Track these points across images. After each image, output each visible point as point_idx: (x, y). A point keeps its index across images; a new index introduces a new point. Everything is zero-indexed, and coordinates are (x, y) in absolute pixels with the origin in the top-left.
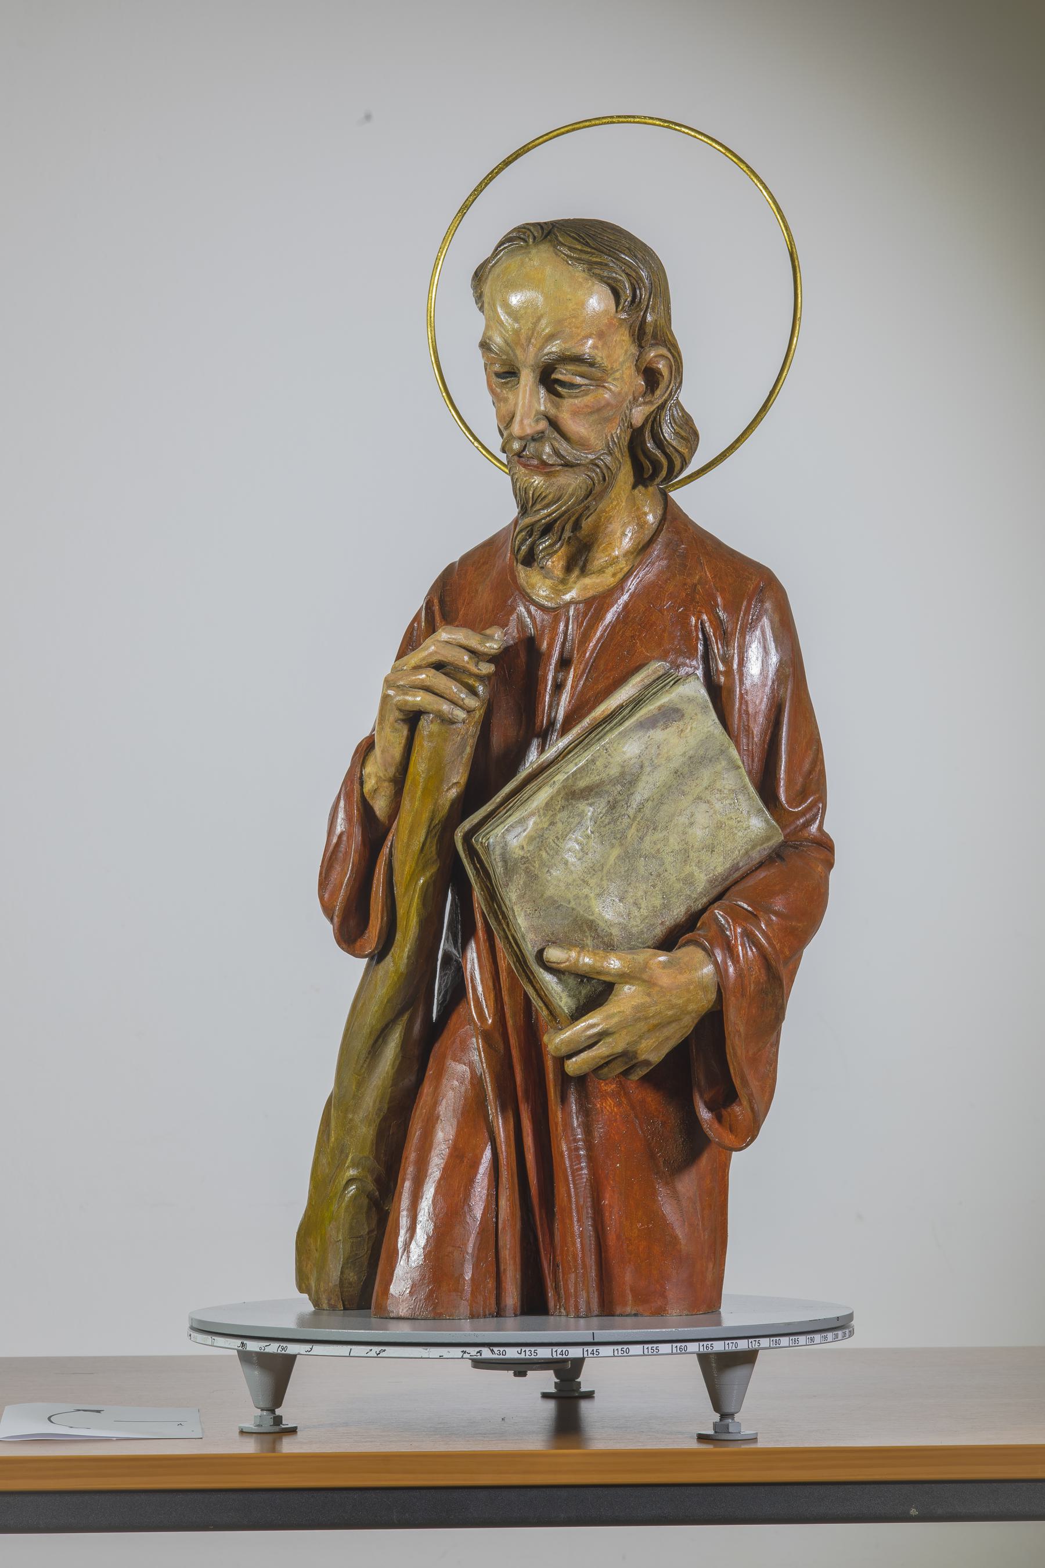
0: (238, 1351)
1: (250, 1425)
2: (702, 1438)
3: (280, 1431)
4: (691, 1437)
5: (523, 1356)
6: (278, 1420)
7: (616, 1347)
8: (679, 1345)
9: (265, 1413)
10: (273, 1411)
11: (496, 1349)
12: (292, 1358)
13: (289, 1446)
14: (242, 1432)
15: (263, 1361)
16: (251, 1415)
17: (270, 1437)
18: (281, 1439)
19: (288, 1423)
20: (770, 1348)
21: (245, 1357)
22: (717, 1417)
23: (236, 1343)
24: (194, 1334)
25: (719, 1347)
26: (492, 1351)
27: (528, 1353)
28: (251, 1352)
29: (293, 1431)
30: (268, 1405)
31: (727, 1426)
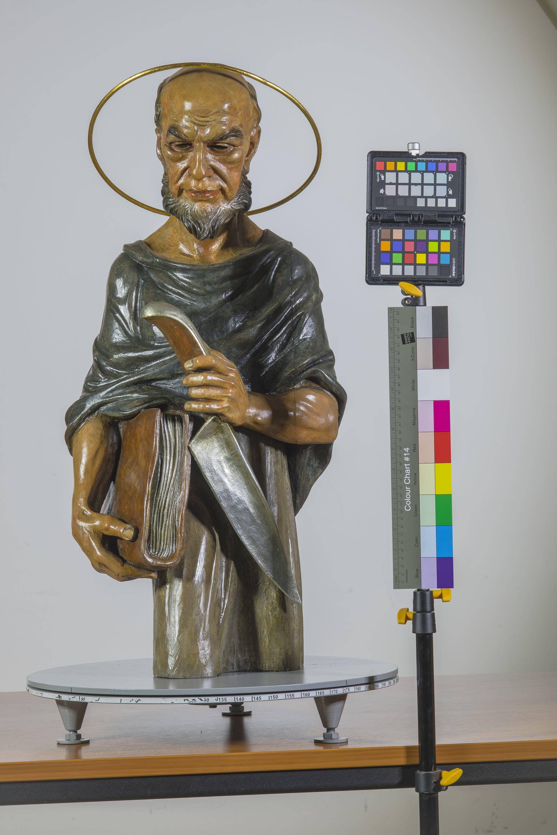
0: (57, 700)
1: (63, 740)
3: (80, 743)
6: (79, 737)
9: (71, 733)
10: (76, 732)
12: (86, 704)
13: (86, 754)
14: (59, 744)
15: (70, 705)
16: (63, 734)
17: (74, 747)
18: (80, 748)
19: (84, 738)
21: (60, 703)
23: (55, 696)
24: (31, 690)
28: (63, 701)
30: (73, 728)
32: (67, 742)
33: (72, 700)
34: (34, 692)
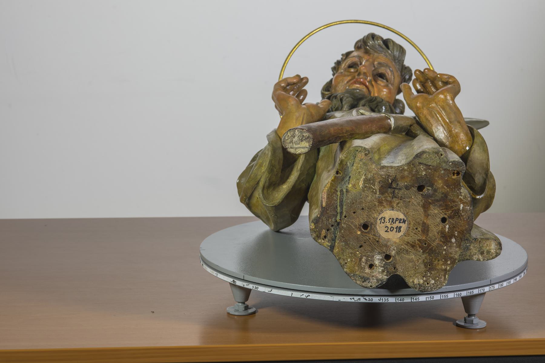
2: (458, 326)
4: (454, 324)
5: (381, 301)
7: (427, 296)
8: (457, 293)
9: (240, 304)
11: (367, 298)
14: (229, 313)
20: (499, 288)
22: (466, 315)
23: (230, 280)
25: (476, 291)
26: (365, 299)
27: (384, 300)
29: (254, 313)
31: (472, 321)
32: (237, 313)
33: (246, 286)
34: (209, 270)
